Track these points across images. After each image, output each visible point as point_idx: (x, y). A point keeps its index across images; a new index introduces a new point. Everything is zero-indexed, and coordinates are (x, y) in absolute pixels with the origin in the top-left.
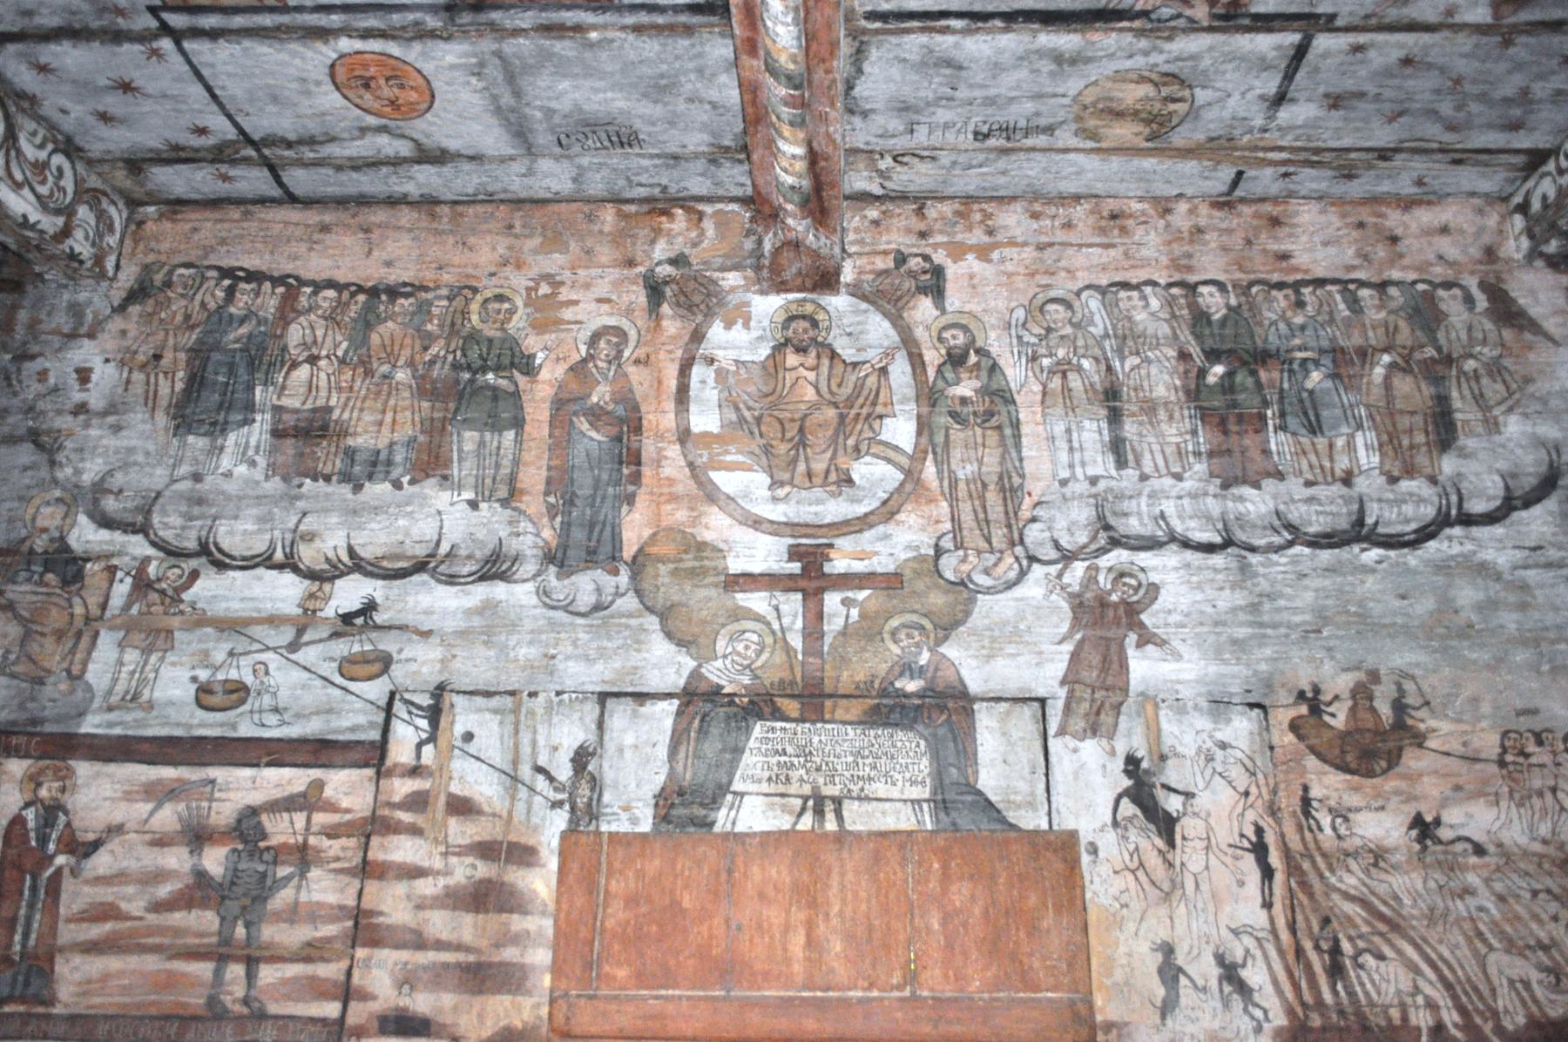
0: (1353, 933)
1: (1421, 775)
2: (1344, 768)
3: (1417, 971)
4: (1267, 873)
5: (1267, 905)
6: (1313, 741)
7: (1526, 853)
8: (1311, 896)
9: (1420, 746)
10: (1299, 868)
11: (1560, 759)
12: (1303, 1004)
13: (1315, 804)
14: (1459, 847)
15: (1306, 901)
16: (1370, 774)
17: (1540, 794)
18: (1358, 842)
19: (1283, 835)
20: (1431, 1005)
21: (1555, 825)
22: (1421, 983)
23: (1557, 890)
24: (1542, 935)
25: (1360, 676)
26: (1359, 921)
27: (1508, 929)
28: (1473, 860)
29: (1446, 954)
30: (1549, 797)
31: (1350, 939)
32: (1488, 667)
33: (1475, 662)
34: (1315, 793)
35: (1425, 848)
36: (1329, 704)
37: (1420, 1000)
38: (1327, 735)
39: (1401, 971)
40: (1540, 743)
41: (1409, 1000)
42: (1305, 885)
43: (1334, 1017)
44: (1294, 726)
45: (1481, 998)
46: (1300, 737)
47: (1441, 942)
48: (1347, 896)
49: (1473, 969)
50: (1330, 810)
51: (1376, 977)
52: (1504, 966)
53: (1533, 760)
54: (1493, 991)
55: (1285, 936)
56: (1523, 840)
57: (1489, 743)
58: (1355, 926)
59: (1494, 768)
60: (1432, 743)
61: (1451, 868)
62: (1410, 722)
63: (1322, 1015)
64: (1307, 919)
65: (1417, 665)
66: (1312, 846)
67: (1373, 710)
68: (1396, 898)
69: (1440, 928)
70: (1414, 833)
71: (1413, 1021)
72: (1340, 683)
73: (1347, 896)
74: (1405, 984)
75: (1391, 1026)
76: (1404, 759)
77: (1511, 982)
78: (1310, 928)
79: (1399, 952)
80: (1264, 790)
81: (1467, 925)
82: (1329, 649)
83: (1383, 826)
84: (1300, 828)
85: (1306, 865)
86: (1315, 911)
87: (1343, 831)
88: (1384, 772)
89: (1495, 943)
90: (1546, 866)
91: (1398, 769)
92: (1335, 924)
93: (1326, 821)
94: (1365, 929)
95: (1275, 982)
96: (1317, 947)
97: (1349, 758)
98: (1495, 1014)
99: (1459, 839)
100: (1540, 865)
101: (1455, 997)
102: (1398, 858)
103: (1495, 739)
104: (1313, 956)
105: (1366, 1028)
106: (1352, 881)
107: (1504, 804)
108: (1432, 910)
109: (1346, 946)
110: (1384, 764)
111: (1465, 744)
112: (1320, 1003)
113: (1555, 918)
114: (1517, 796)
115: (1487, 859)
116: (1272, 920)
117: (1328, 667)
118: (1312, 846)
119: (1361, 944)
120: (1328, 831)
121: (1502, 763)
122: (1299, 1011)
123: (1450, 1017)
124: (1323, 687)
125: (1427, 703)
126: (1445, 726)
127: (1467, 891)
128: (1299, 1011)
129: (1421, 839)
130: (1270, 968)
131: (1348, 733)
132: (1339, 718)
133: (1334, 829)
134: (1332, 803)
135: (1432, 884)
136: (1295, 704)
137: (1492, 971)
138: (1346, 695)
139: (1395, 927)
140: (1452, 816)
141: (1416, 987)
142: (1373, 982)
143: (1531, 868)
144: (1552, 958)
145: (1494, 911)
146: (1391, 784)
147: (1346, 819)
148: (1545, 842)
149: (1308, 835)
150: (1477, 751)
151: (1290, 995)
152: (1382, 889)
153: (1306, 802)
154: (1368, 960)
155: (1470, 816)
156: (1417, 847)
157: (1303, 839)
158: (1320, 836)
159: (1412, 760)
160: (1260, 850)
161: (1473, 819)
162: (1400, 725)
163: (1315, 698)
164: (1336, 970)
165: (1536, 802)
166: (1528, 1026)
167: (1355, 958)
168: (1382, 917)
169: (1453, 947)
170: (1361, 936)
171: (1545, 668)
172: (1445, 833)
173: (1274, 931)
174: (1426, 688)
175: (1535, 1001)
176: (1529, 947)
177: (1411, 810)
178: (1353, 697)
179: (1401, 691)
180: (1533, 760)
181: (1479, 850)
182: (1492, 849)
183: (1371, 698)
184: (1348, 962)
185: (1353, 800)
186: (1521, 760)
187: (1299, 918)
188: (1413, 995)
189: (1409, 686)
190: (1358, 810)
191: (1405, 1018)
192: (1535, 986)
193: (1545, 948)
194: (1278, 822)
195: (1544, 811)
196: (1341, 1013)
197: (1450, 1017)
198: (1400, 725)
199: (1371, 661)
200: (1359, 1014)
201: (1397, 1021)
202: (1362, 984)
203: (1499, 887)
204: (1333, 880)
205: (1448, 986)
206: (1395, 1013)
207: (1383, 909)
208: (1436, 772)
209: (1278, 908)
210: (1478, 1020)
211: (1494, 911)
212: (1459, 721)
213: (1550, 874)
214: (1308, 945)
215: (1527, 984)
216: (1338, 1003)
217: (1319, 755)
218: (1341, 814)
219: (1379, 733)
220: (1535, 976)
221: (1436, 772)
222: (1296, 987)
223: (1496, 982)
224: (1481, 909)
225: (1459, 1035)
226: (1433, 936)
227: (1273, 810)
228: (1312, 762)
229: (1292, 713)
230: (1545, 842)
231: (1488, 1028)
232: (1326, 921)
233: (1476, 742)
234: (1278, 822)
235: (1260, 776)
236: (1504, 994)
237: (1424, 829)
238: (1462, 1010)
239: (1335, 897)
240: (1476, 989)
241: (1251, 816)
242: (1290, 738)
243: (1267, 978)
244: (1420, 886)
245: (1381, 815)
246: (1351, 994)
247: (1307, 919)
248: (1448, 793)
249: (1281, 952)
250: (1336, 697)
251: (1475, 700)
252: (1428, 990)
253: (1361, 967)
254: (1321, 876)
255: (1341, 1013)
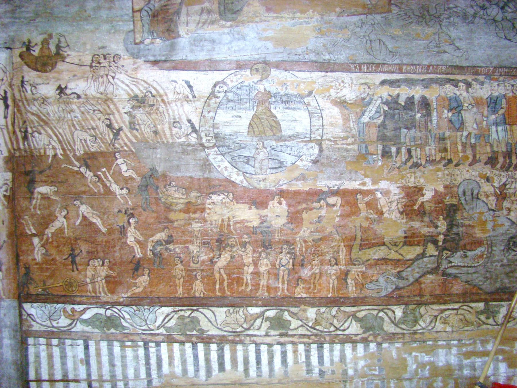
0: (32, 126)
1: (63, 72)
2: (36, 70)
3: (51, 137)
4: (7, 106)
5: (6, 117)
6: (27, 61)
7: (94, 97)
8: (21, 114)
9: (63, 61)
10: (18, 105)
11: (111, 64)
12: (14, 149)
13: (26, 83)
14: (72, 96)
15: (19, 115)
16: (46, 72)
17: (102, 77)
18: (39, 95)
19: (14, 94)
20: (54, 148)
21: (106, 87)
22: (52, 141)
23: (101, 110)
24: (94, 125)
25: (46, 36)
26: (35, 122)
27: (83, 123)
28: (75, 100)
29: (61, 131)
30: (105, 77)
31: (31, 128)
32: (92, 31)
33: (87, 30)
34: (26, 79)
35: (61, 97)
36: (33, 47)
37: (51, 147)
38: (31, 57)
39: (46, 137)
40: (105, 59)
41: (47, 147)
42: (19, 111)
43: (23, 153)
44: (21, 56)
45: (70, 145)
46: (22, 59)
47: (60, 128)
48: (33, 114)
49: (69, 137)
50: (31, 85)
51: (38, 140)
52: (80, 135)
53: (102, 65)
54: (75, 143)
55: (10, 127)
56: (94, 93)
57: (87, 59)
58: (34, 124)
59: (88, 68)
60: (67, 60)
61: (67, 103)
62: (61, 52)
63: (20, 153)
64: (19, 122)
65: (66, 31)
66: (23, 97)
67: (49, 48)
68: (48, 114)
69: (61, 124)
70: (58, 92)
71: (48, 153)
72: (37, 39)
73: (33, 114)
74: (46, 142)
75: (41, 156)
76: (57, 66)
77: (81, 140)
78: (19, 125)
79: (46, 131)
80: (9, 79)
81: (70, 122)
82: (37, 27)
83: (48, 90)
84: (20, 91)
85: (20, 104)
86: (22, 119)
87: (34, 92)
88: (50, 71)
89: (78, 128)
90: (100, 102)
91: (55, 70)
92: (27, 123)
93: (28, 88)
94: (36, 124)
95: (6, 143)
96: (20, 131)
97: (38, 66)
98: (74, 150)
99: (73, 93)
100: (97, 101)
101: (62, 146)
102: (51, 100)
103: (90, 58)
104: (19, 134)
105: (32, 156)
106: (35, 108)
107: (89, 81)
108: (59, 117)
109: (30, 130)
110: (50, 68)
111: (80, 60)
112: (19, 149)
113: (99, 119)
114: (94, 78)
115: (80, 100)
116: (7, 122)
117: (35, 34)
118: (23, 97)
119: (34, 129)
120: (29, 92)
121: (91, 66)
122: (13, 151)
123: (59, 152)
124: (32, 41)
125: (68, 46)
126: (72, 53)
127: (72, 111)
128: (13, 151)
129: (60, 94)
130: (4, 138)
131: (39, 57)
132: (36, 52)
133: (31, 91)
134: (31, 82)
135: (60, 109)
136: (22, 47)
137: (75, 136)
138: (40, 43)
139: (46, 123)
140: (72, 86)
141: (50, 143)
142: (36, 142)
143: (94, 103)
144: (95, 132)
145: (80, 117)
146: (51, 75)
147: (36, 88)
148: (101, 93)
149: (22, 93)
150: (83, 62)
151: (10, 146)
152: (44, 111)
153: (23, 82)
154: (36, 134)
155: (77, 85)
156: (58, 96)
157: (21, 95)
158: (27, 94)
159: (60, 66)
160: (5, 99)
161: (78, 86)
162: (58, 54)
163: (29, 45)
164: (25, 138)
165: (100, 79)
166: (84, 154)
167: (32, 134)
168: (43, 121)
169: (64, 130)
170: (34, 127)
171: (113, 31)
172: (68, 92)
173: (7, 126)
174: (69, 41)
175: (88, 146)
176: (89, 129)
177: (57, 84)
178: (42, 44)
179: (59, 41)
180: (102, 65)
181: (79, 97)
182: (83, 96)
183: (48, 44)
184: (29, 135)
185: (39, 81)
186: (98, 65)
187: (16, 121)
188: (48, 145)
189: (62, 39)
190: (40, 84)
191: (45, 153)
192: (88, 142)
193: (94, 129)
194: (13, 90)
195: (103, 83)
196: (26, 151)
197: (59, 152)
198: (58, 54)
199: (50, 31)
200: (31, 151)
201: (43, 154)
202: (33, 142)
203: (82, 109)
204: (29, 109)
205: (60, 142)
206: (42, 151)
207: (44, 118)
208: (68, 70)
209: (9, 119)
210: (68, 152)
211: (80, 117)
212: (78, 52)
213: (100, 104)
214: (17, 130)
215: (85, 140)
216: (25, 148)
217: (29, 66)
218: (34, 86)
219: (49, 57)
220: (89, 138)
221: (68, 70)
222: (12, 143)
223: (76, 140)
224: (75, 117)
225: (62, 157)
226: (58, 126)
227: (11, 85)
228: (25, 68)
229: (20, 50)
230: (101, 93)
231: (71, 155)
232: (25, 122)
233: (83, 59)
234: (13, 90)
235: (8, 73)
236: (78, 143)
237: (61, 90)
238: (64, 150)
239: (29, 114)
240: (69, 143)
241: (3, 87)
242: (19, 59)
243: (3, 141)
244: (57, 110)
245: (48, 86)
246: (29, 145)
247: (19, 122)
248: (71, 77)
249: (8, 132)
250: (36, 44)
251: (84, 44)
252: (54, 143)
253: (33, 137)
254: (25, 107)
255: (26, 151)
